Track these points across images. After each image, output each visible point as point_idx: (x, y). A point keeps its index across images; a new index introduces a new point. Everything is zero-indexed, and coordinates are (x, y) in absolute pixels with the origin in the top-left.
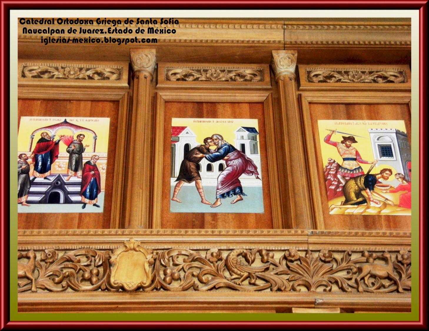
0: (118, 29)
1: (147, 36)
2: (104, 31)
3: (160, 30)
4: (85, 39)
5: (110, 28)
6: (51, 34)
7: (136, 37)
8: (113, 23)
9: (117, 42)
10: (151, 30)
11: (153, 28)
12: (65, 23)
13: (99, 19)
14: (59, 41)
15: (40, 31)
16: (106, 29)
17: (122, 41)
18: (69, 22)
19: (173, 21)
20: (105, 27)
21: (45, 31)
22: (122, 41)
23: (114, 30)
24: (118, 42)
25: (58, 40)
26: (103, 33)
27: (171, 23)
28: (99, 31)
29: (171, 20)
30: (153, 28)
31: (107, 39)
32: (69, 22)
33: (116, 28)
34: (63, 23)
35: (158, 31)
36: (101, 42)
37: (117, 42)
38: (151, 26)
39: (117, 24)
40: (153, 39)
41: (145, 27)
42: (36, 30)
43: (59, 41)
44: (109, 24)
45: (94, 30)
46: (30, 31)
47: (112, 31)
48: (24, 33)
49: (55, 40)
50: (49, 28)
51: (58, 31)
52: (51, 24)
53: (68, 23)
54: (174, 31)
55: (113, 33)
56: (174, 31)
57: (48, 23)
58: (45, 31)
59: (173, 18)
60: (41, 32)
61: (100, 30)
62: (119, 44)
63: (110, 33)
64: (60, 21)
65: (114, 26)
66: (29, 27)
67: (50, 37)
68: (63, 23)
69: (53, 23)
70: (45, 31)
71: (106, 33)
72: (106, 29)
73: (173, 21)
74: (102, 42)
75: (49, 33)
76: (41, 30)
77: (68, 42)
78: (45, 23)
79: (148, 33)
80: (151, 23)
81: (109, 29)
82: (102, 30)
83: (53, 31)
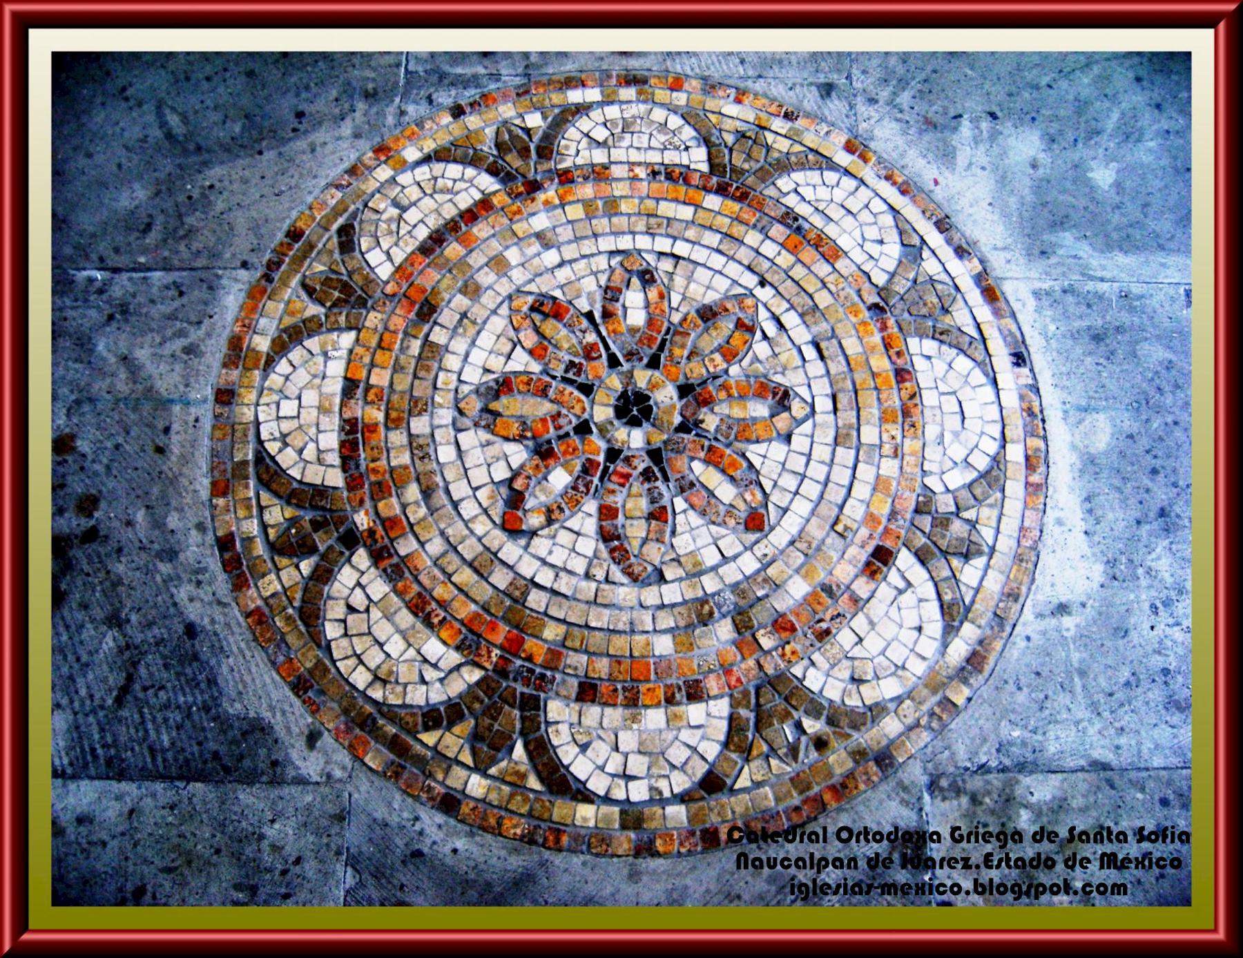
0: (1013, 856)
1: (1097, 874)
2: (972, 861)
3: (1137, 859)
4: (917, 885)
5: (990, 854)
6: (819, 872)
7: (1065, 880)
8: (999, 840)
9: (1010, 896)
10: (1109, 860)
11: (1114, 855)
12: (858, 841)
13: (959, 828)
14: (841, 890)
15: (786, 863)
16: (976, 857)
17: (1024, 888)
18: (870, 837)
19: (1173, 834)
20: (977, 852)
21: (800, 862)
22: (1024, 888)
23: (1000, 861)
24: (1013, 892)
25: (839, 886)
26: (970, 867)
27: (1168, 840)
28: (957, 862)
29: (1169, 833)
30: (1114, 855)
31: (982, 885)
32: (870, 837)
33: (1007, 854)
34: (854, 839)
35: (1130, 861)
36: (963, 893)
37: (1010, 896)
38: (1108, 848)
39: (1010, 841)
40: (1114, 885)
41: (1092, 850)
42: (775, 859)
43: (841, 890)
44: (989, 842)
45: (943, 860)
46: (758, 864)
47: (995, 863)
48: (739, 867)
49: (829, 886)
50: (812, 855)
51: (838, 863)
52: (818, 841)
53: (867, 841)
54: (1176, 863)
55: (998, 866)
56: (1176, 863)
57: (811, 841)
58: (801, 863)
59: (1173, 827)
60: (789, 866)
61: (962, 859)
62: (1015, 899)
63: (991, 867)
64: (844, 835)
65: (1001, 847)
66: (753, 851)
67: (814, 881)
68: (854, 839)
69: (825, 841)
70: (801, 863)
71: (978, 867)
72: (976, 857)
73: (1173, 834)
74: (968, 893)
75: (812, 868)
76: (789, 860)
77: (868, 893)
78: (802, 841)
79: (1102, 867)
80: (1110, 841)
81: (988, 857)
82: (966, 860)
83: (822, 864)
